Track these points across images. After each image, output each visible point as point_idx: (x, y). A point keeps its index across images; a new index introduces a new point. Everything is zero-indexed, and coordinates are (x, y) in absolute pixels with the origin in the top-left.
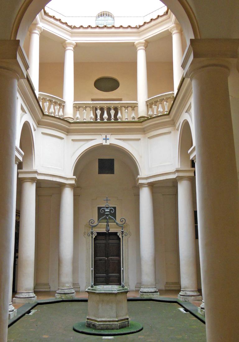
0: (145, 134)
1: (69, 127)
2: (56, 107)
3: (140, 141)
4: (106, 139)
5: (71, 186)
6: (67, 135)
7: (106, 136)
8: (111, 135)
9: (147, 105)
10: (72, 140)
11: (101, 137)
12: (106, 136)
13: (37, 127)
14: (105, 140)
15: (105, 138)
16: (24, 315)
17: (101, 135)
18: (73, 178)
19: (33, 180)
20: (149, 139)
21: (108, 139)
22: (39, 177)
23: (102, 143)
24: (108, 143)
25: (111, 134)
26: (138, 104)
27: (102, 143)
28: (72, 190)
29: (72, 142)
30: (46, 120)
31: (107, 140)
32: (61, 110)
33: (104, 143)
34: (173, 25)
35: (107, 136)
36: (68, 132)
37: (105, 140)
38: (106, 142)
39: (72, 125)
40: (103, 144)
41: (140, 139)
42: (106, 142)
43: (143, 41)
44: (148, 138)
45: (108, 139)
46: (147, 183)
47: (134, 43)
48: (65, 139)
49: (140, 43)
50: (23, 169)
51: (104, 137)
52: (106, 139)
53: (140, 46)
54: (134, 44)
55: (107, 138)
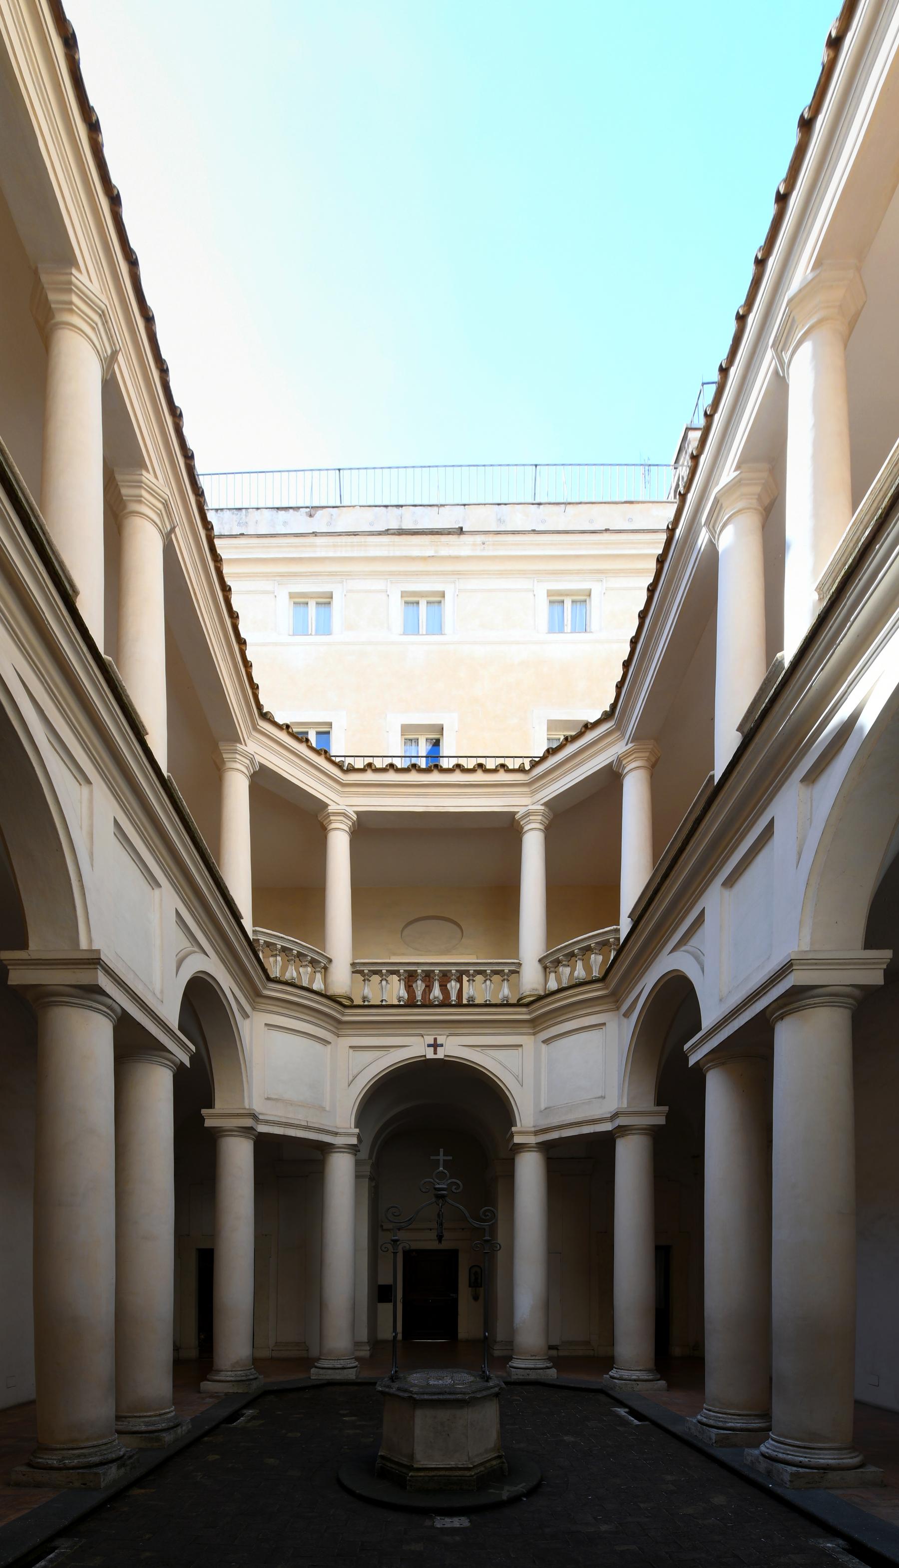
4: (435, 1046)
7: (435, 1039)
8: (448, 1036)
12: (435, 1039)
14: (432, 1049)
15: (432, 1042)
17: (422, 1036)
19: (247, 1131)
21: (442, 1045)
22: (262, 1129)
23: (425, 1056)
24: (440, 1054)
27: (425, 1056)
31: (438, 1048)
33: (430, 1055)
37: (432, 1049)
38: (435, 1053)
40: (428, 1057)
42: (435, 1053)
44: (544, 1042)
45: (442, 1045)
48: (332, 1043)
52: (435, 1046)
55: (439, 1042)
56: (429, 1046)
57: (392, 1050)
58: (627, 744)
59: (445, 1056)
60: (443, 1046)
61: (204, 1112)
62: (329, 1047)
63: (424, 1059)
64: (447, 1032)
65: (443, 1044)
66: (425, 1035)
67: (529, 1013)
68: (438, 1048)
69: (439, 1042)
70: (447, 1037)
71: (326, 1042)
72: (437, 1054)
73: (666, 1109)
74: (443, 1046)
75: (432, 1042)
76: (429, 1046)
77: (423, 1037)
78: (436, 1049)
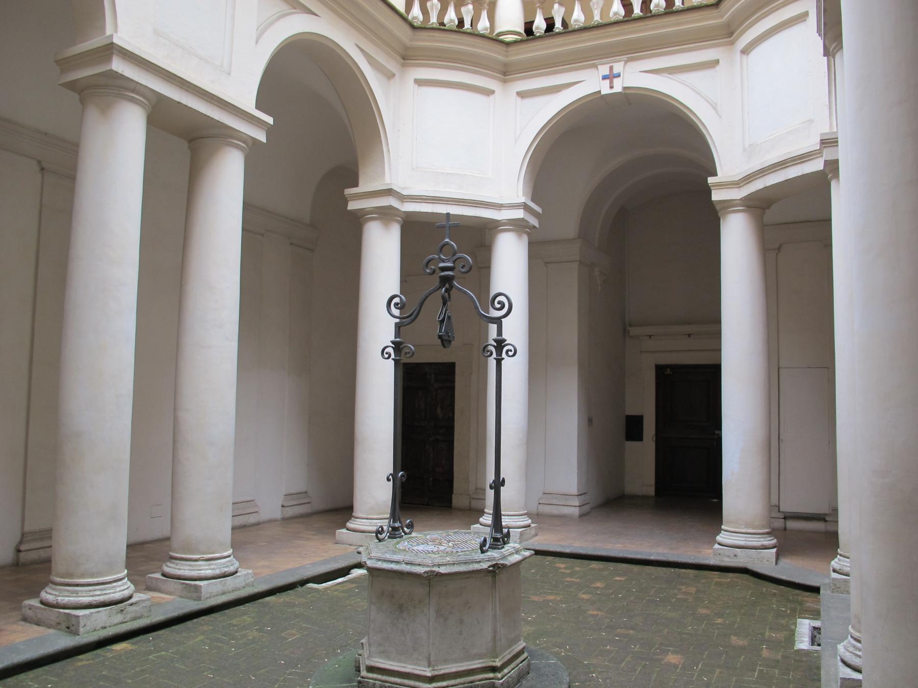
1: (506, 56)
2: (463, 9)
3: (718, 68)
4: (610, 77)
5: (518, 226)
6: (505, 81)
7: (611, 68)
8: (626, 62)
12: (611, 68)
13: (403, 65)
14: (607, 81)
16: (303, 583)
17: (595, 66)
24: (618, 88)
28: (520, 236)
29: (519, 99)
30: (425, 41)
32: (484, 15)
33: (606, 90)
36: (506, 73)
38: (611, 87)
39: (512, 49)
40: (603, 93)
41: (716, 62)
42: (611, 87)
50: (361, 181)
51: (604, 70)
52: (610, 77)
55: (615, 71)
56: (604, 78)
59: (625, 88)
60: (619, 76)
61: (349, 191)
62: (492, 97)
63: (598, 96)
64: (625, 57)
65: (620, 73)
68: (615, 80)
69: (615, 71)
71: (489, 92)
75: (607, 72)
76: (604, 78)
77: (597, 68)
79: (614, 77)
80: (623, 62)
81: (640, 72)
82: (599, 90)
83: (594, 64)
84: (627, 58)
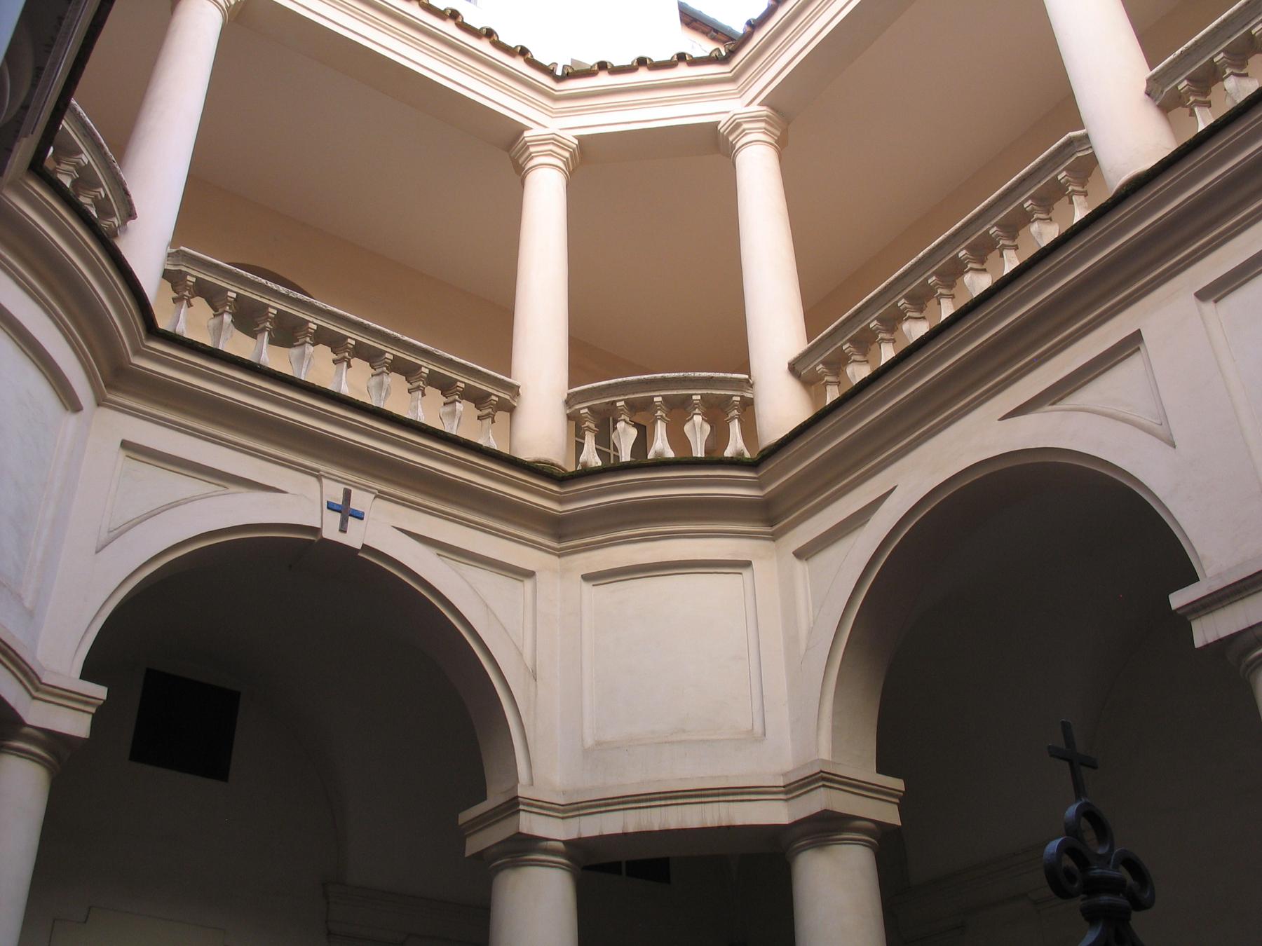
0: (560, 554)
4: (346, 511)
7: (347, 495)
8: (377, 497)
9: (571, 417)
10: (125, 445)
11: (317, 484)
12: (347, 495)
15: (339, 500)
17: (318, 476)
18: (85, 699)
20: (587, 587)
21: (359, 516)
23: (315, 531)
24: (354, 537)
25: (380, 495)
26: (518, 394)
33: (331, 532)
34: (755, 107)
35: (354, 491)
38: (343, 530)
42: (343, 530)
43: (570, 138)
45: (359, 516)
46: (565, 842)
47: (524, 128)
49: (555, 140)
51: (335, 492)
53: (551, 154)
54: (522, 132)
55: (354, 505)
56: (331, 507)
57: (233, 489)
58: (748, 105)
59: (364, 545)
60: (362, 519)
65: (363, 513)
66: (326, 477)
67: (561, 501)
69: (354, 505)
70: (375, 498)
72: (345, 532)
73: (898, 784)
74: (362, 519)
75: (339, 500)
78: (347, 521)
79: (351, 515)
80: (374, 496)
81: (394, 527)
82: (319, 526)
83: (318, 471)
84: (379, 491)
